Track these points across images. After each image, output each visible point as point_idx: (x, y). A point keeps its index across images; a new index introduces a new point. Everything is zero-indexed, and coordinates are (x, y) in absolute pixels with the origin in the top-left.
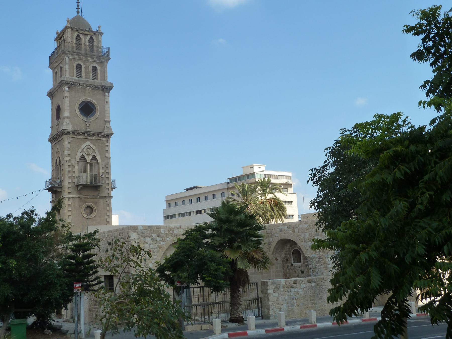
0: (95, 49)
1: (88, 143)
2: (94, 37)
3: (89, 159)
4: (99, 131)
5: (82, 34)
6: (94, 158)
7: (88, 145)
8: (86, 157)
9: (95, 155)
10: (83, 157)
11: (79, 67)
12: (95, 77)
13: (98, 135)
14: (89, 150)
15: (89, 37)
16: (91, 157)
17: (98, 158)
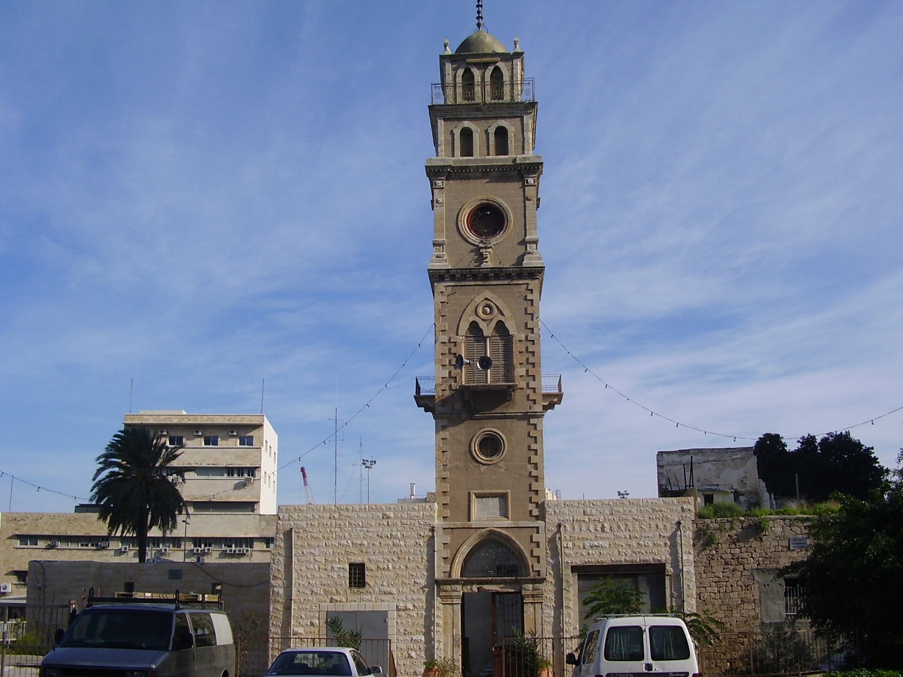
0: (507, 89)
1: (488, 294)
2: (502, 65)
3: (488, 330)
4: (508, 263)
5: (476, 65)
6: (501, 327)
7: (486, 299)
8: (482, 325)
9: (502, 319)
10: (474, 328)
11: (467, 135)
12: (502, 148)
13: (508, 276)
14: (488, 310)
15: (491, 68)
16: (493, 324)
17: (511, 326)
